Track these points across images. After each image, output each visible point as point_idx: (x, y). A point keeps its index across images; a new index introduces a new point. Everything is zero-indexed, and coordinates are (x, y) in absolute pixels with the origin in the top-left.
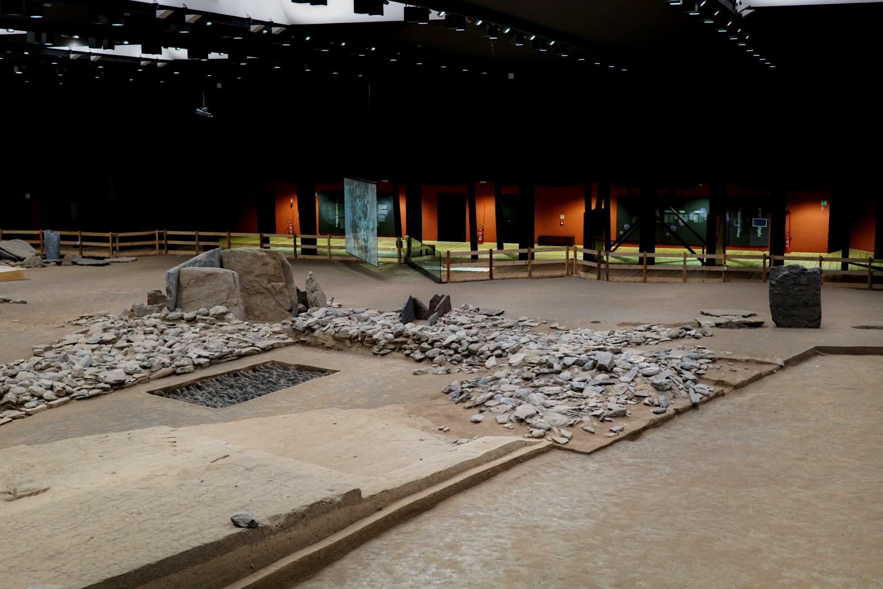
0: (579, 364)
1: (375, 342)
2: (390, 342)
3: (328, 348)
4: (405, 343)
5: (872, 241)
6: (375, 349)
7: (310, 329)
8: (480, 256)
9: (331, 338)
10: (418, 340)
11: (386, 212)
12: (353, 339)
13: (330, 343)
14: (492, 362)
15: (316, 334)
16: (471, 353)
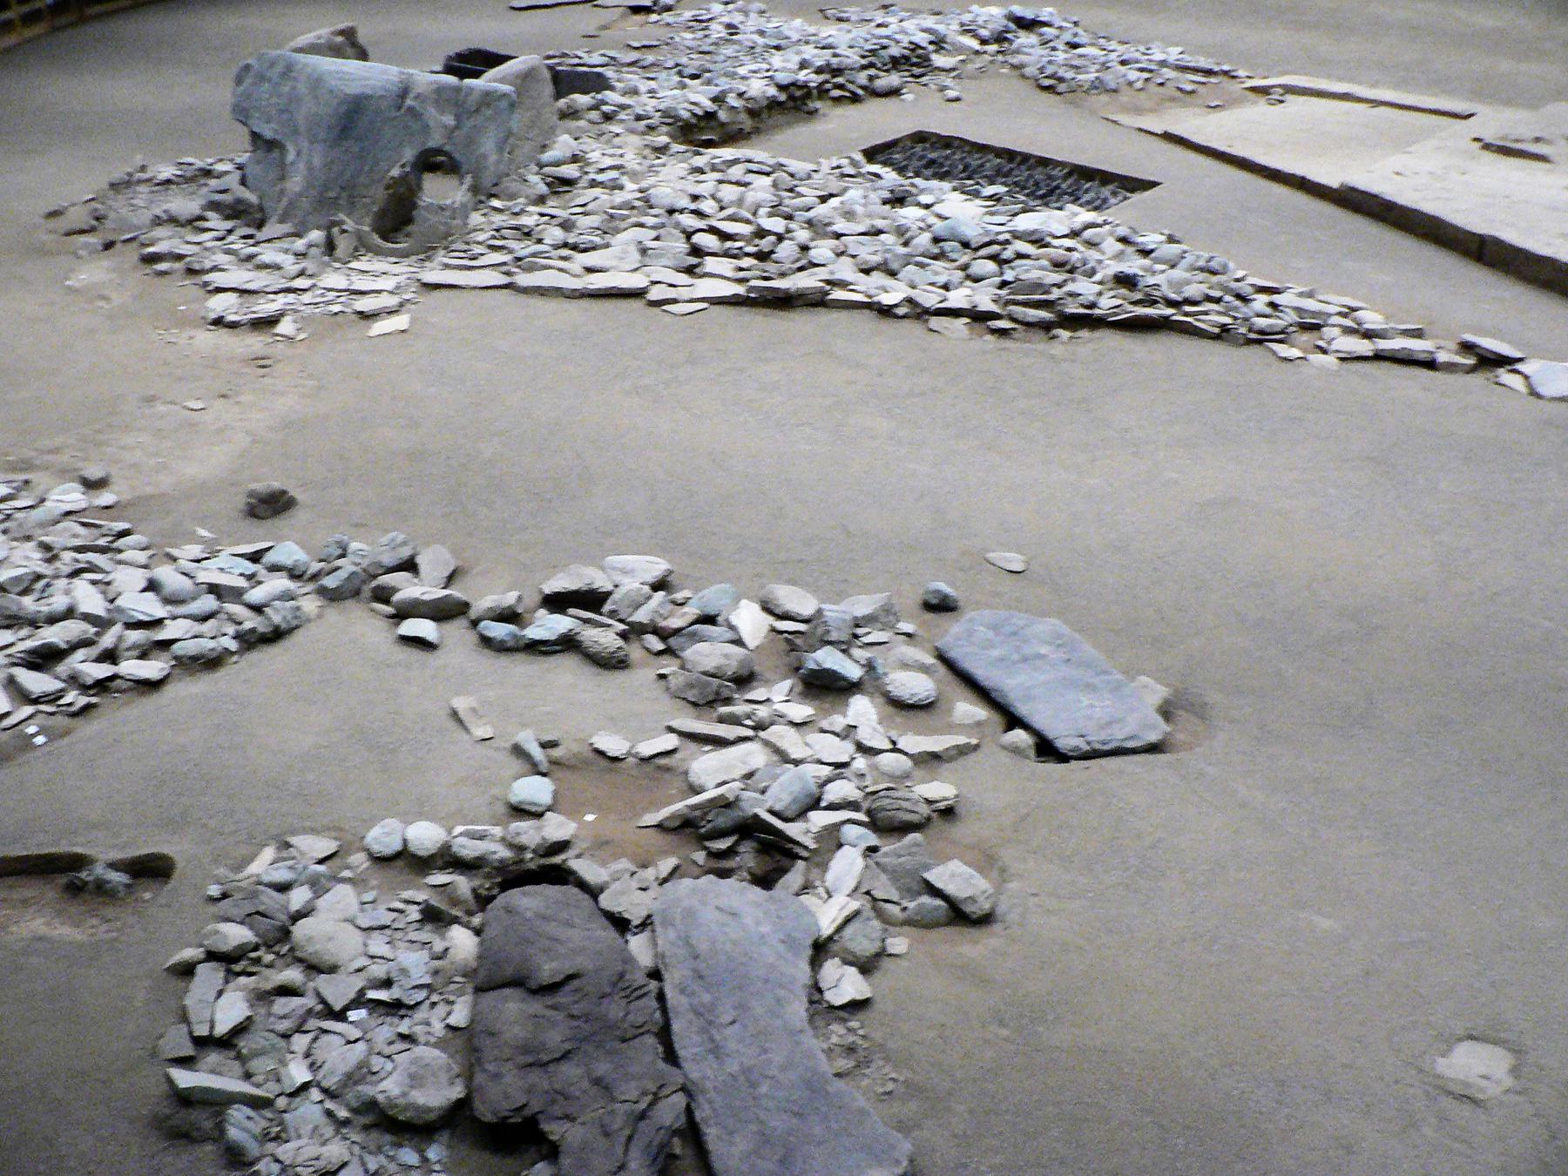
9: (743, 117)
13: (747, 123)
14: (939, 60)
15: (723, 115)
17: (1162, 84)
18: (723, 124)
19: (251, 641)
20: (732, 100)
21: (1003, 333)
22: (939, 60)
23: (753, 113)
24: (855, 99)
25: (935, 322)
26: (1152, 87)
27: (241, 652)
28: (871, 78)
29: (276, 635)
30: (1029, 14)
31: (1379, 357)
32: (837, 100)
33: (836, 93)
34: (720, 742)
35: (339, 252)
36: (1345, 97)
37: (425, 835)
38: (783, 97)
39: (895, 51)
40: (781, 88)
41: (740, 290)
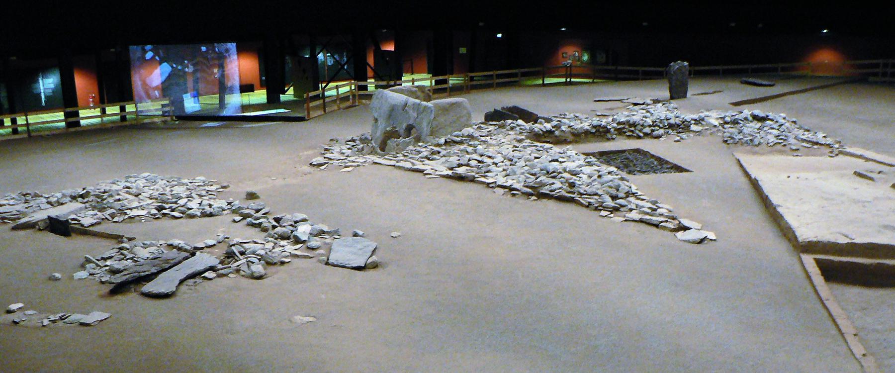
0: (746, 119)
1: (608, 131)
2: (616, 129)
3: (570, 143)
4: (624, 128)
5: (426, 66)
6: (609, 136)
7: (550, 132)
8: (19, 129)
10: (634, 125)
11: (52, 86)
12: (587, 133)
13: (570, 138)
14: (694, 127)
15: (557, 133)
16: (671, 126)
17: (785, 145)
18: (556, 136)
19: (205, 215)
20: (563, 128)
21: (514, 195)
22: (694, 127)
23: (574, 134)
24: (639, 137)
25: (497, 189)
26: (779, 147)
27: (200, 217)
28: (653, 131)
29: (211, 215)
30: (762, 114)
31: (641, 221)
32: (629, 137)
33: (628, 134)
34: (256, 243)
35: (364, 152)
36: (860, 157)
37: (176, 242)
38: (594, 131)
39: (672, 121)
40: (594, 127)
41: (450, 173)
